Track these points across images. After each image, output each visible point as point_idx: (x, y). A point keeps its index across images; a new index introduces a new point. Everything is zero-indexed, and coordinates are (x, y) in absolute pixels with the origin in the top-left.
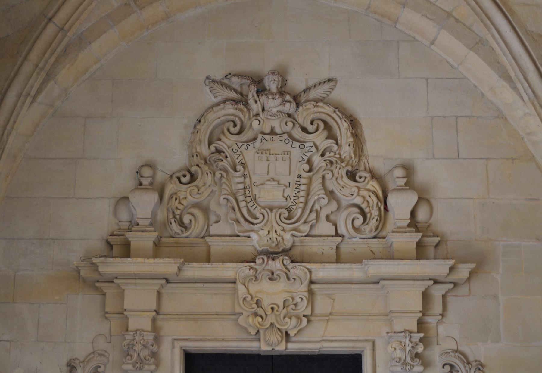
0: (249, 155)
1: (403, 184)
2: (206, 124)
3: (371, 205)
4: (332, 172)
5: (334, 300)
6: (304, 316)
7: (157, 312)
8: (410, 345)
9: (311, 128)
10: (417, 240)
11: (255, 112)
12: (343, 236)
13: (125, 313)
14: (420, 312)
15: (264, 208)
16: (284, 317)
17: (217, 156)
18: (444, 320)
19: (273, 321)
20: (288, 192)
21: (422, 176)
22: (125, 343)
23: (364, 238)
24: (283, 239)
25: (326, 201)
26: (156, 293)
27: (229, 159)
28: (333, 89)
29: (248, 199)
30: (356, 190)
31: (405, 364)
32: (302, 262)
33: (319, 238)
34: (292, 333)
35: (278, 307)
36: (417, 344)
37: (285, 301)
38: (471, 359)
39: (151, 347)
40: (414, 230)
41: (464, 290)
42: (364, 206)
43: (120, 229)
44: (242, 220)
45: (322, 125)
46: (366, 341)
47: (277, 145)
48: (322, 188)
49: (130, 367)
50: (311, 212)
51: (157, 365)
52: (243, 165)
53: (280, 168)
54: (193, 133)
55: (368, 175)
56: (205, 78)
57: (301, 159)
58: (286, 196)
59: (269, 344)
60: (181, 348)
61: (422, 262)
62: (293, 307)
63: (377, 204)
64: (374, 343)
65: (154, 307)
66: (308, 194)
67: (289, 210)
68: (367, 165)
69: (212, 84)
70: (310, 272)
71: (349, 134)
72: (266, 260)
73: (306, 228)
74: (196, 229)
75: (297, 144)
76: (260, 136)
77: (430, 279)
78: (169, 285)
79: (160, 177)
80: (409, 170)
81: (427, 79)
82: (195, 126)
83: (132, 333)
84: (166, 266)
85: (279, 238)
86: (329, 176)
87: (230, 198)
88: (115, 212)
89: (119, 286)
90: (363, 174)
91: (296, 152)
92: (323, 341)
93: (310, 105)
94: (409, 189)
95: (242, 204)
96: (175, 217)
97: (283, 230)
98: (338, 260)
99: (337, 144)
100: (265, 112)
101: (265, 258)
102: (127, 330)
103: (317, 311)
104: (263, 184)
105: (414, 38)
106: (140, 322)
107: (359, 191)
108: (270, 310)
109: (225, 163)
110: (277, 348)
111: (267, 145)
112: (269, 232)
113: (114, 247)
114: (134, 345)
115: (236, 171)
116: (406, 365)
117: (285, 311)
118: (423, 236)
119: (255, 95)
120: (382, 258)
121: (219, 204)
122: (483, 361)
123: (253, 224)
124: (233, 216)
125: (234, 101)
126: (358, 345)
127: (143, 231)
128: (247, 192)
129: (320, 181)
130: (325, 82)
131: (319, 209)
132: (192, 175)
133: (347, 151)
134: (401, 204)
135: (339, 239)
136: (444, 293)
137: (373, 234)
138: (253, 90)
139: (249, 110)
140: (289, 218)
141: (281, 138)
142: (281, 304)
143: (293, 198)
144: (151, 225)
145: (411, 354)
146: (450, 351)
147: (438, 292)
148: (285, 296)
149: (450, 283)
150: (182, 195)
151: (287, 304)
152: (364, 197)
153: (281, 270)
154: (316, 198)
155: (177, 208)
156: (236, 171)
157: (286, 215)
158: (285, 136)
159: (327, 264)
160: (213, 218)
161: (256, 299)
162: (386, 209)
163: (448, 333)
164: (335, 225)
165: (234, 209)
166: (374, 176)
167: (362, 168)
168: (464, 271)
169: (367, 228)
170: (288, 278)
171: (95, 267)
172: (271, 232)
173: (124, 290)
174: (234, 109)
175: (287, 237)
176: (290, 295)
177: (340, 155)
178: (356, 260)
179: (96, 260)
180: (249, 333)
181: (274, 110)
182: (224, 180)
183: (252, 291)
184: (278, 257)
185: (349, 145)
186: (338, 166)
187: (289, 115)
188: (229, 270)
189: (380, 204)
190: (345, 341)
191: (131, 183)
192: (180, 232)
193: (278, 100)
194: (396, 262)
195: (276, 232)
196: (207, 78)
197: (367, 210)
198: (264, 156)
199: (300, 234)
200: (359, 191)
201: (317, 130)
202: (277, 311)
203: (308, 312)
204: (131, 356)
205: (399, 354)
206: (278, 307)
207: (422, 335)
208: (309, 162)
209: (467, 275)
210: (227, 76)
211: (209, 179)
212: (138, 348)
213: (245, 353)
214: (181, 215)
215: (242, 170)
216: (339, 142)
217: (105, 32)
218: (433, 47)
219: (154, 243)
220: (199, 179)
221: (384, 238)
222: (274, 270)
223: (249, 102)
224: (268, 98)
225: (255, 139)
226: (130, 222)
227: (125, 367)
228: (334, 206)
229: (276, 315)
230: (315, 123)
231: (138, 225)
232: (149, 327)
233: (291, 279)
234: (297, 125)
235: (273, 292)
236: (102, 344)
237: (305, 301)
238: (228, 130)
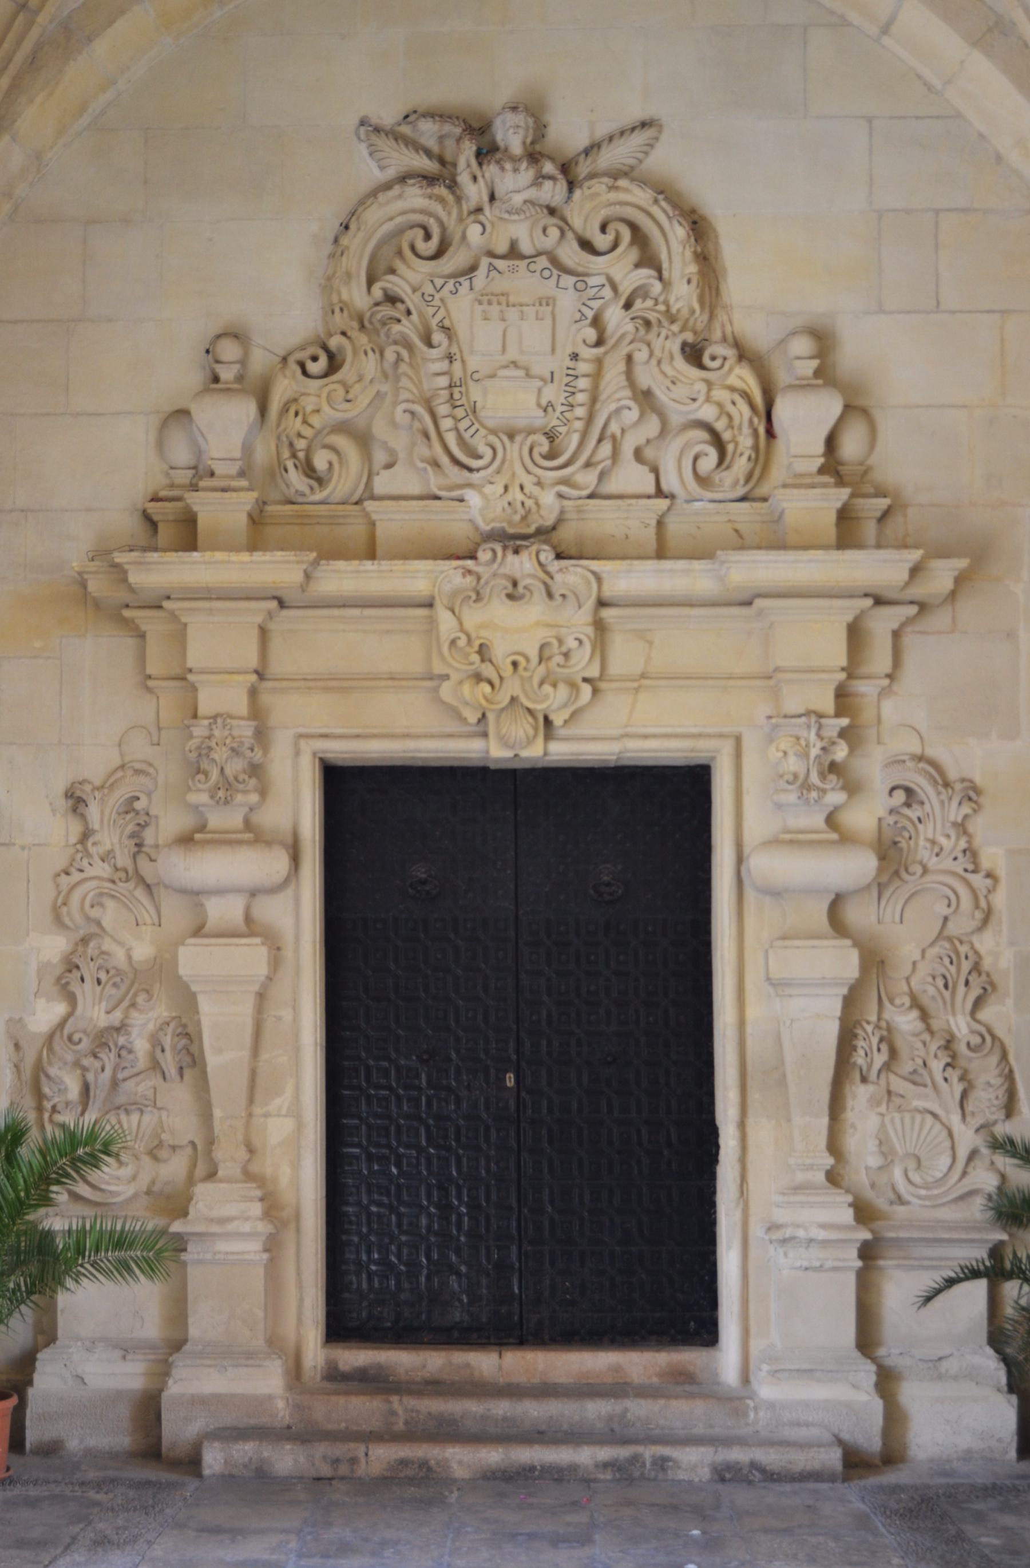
0: (461, 307)
1: (810, 372)
2: (361, 234)
3: (736, 422)
4: (649, 345)
5: (650, 643)
6: (585, 680)
7: (260, 675)
8: (819, 744)
9: (601, 241)
10: (839, 505)
11: (473, 204)
12: (672, 497)
13: (191, 677)
14: (843, 669)
15: (494, 432)
16: (541, 684)
17: (386, 310)
18: (895, 688)
19: (517, 691)
20: (550, 393)
21: (852, 354)
22: (193, 744)
23: (720, 501)
24: (537, 504)
25: (634, 414)
26: (255, 632)
27: (415, 317)
28: (651, 146)
29: (460, 413)
30: (702, 387)
31: (806, 786)
32: (580, 558)
33: (619, 502)
34: (558, 720)
35: (528, 660)
36: (834, 743)
37: (542, 647)
38: (953, 775)
39: (249, 754)
40: (832, 480)
41: (941, 619)
42: (720, 426)
43: (172, 486)
44: (445, 460)
45: (626, 234)
46: (721, 736)
47: (523, 282)
48: (625, 383)
49: (204, 798)
50: (600, 440)
51: (263, 792)
52: (446, 330)
53: (532, 337)
54: (332, 256)
55: (730, 353)
56: (356, 122)
57: (578, 316)
58: (544, 402)
59: (510, 744)
60: (314, 754)
61: (850, 554)
62: (559, 659)
63: (751, 421)
64: (738, 740)
65: (253, 662)
66: (594, 400)
67: (551, 436)
68: (728, 329)
69: (374, 138)
70: (599, 579)
71: (689, 254)
72: (500, 554)
73: (588, 479)
74: (344, 483)
75: (568, 281)
76: (485, 262)
77: (866, 595)
78: (285, 613)
79: (260, 361)
80: (823, 340)
81: (870, 120)
82: (336, 240)
83: (206, 722)
84: (278, 569)
85: (529, 503)
86: (641, 356)
87: (420, 409)
88: (160, 445)
89: (174, 617)
90: (720, 350)
91: (567, 301)
92: (627, 735)
93: (599, 186)
94: (825, 385)
95: (446, 424)
96: (294, 456)
97: (539, 483)
98: (661, 554)
99: (660, 278)
100: (497, 203)
101: (498, 548)
102: (195, 716)
103: (615, 668)
104: (493, 376)
105: (842, 17)
106: (224, 697)
107: (709, 390)
108: (510, 668)
109: (407, 328)
110: (525, 753)
111: (501, 284)
112: (506, 488)
113: (161, 527)
114: (210, 749)
115: (430, 344)
116: (809, 790)
117: (542, 670)
118: (853, 495)
119: (474, 163)
120: (759, 548)
121: (393, 424)
122: (978, 780)
123: (470, 470)
124: (423, 450)
125: (425, 177)
126: (702, 744)
127: (224, 490)
128: (457, 396)
129: (622, 367)
130: (633, 129)
131: (618, 433)
132: (331, 356)
133: (683, 294)
134: (805, 421)
135: (663, 504)
136: (895, 625)
137: (740, 491)
138: (469, 148)
139: (459, 199)
140: (551, 456)
141: (532, 267)
142: (533, 654)
143: (560, 409)
144: (242, 474)
145: (820, 764)
146: (905, 758)
147: (882, 624)
148: (543, 634)
149: (912, 603)
150: (308, 404)
151: (547, 653)
152: (720, 405)
153: (534, 576)
154: (613, 406)
155: (300, 435)
156: (430, 344)
157: (545, 447)
158: (543, 262)
159: (636, 562)
160: (380, 457)
161: (477, 643)
162: (770, 433)
163: (904, 718)
164: (655, 470)
165: (427, 436)
166: (744, 354)
167: (718, 335)
168: (942, 576)
169: (727, 477)
170: (550, 595)
171: (119, 573)
172: (510, 489)
173: (185, 625)
174: (424, 196)
175: (548, 498)
176: (553, 632)
177: (668, 306)
178: (702, 551)
179: (120, 558)
180: (464, 720)
181: (518, 199)
182: (404, 368)
183: (469, 623)
184: (527, 547)
185: (689, 282)
186: (664, 332)
187: (552, 211)
188: (417, 578)
189: (756, 420)
190: (676, 736)
191: (196, 378)
192: (307, 491)
193: (526, 174)
194: (791, 555)
195: (522, 488)
196: (363, 123)
197: (726, 436)
198: (494, 310)
199: (575, 493)
200: (709, 390)
201: (615, 246)
202: (525, 669)
203: (594, 672)
204: (206, 774)
205: (793, 764)
206: (528, 660)
207: (845, 722)
208: (597, 322)
209: (948, 584)
210: (406, 117)
211: (370, 365)
212: (220, 754)
213: (456, 764)
214: (308, 451)
215: (445, 342)
216: (665, 274)
217: (122, 12)
218: (886, 40)
219: (250, 516)
221: (765, 500)
222: (518, 575)
223: (459, 179)
224: (502, 169)
225: (473, 268)
226: (195, 468)
227: (193, 798)
228: (652, 426)
229: (522, 679)
230: (611, 228)
231: (212, 474)
232: (243, 709)
233: (557, 596)
234: (570, 235)
235: (516, 627)
236: (139, 749)
237: (588, 646)
238: (413, 248)
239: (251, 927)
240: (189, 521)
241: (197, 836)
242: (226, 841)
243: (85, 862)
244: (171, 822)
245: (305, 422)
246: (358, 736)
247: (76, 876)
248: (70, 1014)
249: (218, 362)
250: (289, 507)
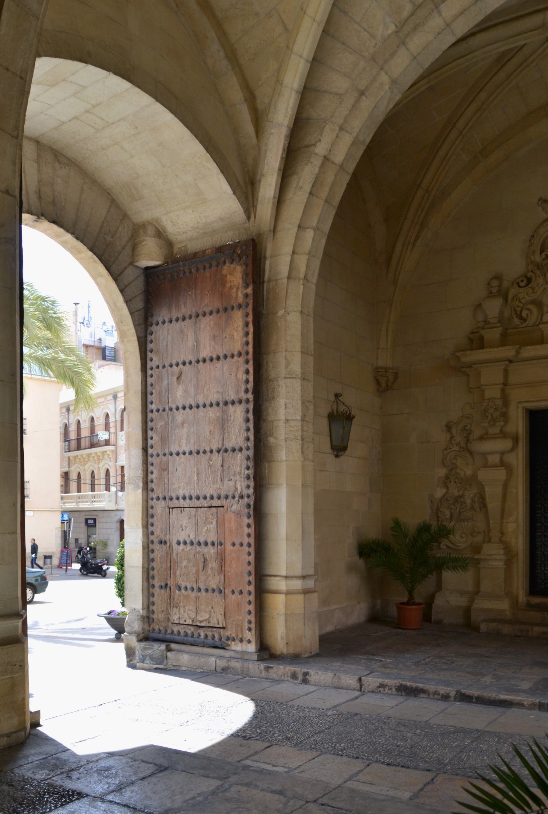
60: (523, 408)
65: (501, 379)
74: (531, 321)
78: (512, 364)
96: (516, 313)
144: (499, 321)
155: (518, 306)
220: (533, 282)
239: (502, 464)
240: (482, 338)
241: (485, 436)
242: (494, 437)
243: (451, 446)
244: (477, 433)
245: (520, 302)
246: (538, 401)
247: (449, 451)
248: (447, 492)
249: (492, 287)
250: (515, 330)
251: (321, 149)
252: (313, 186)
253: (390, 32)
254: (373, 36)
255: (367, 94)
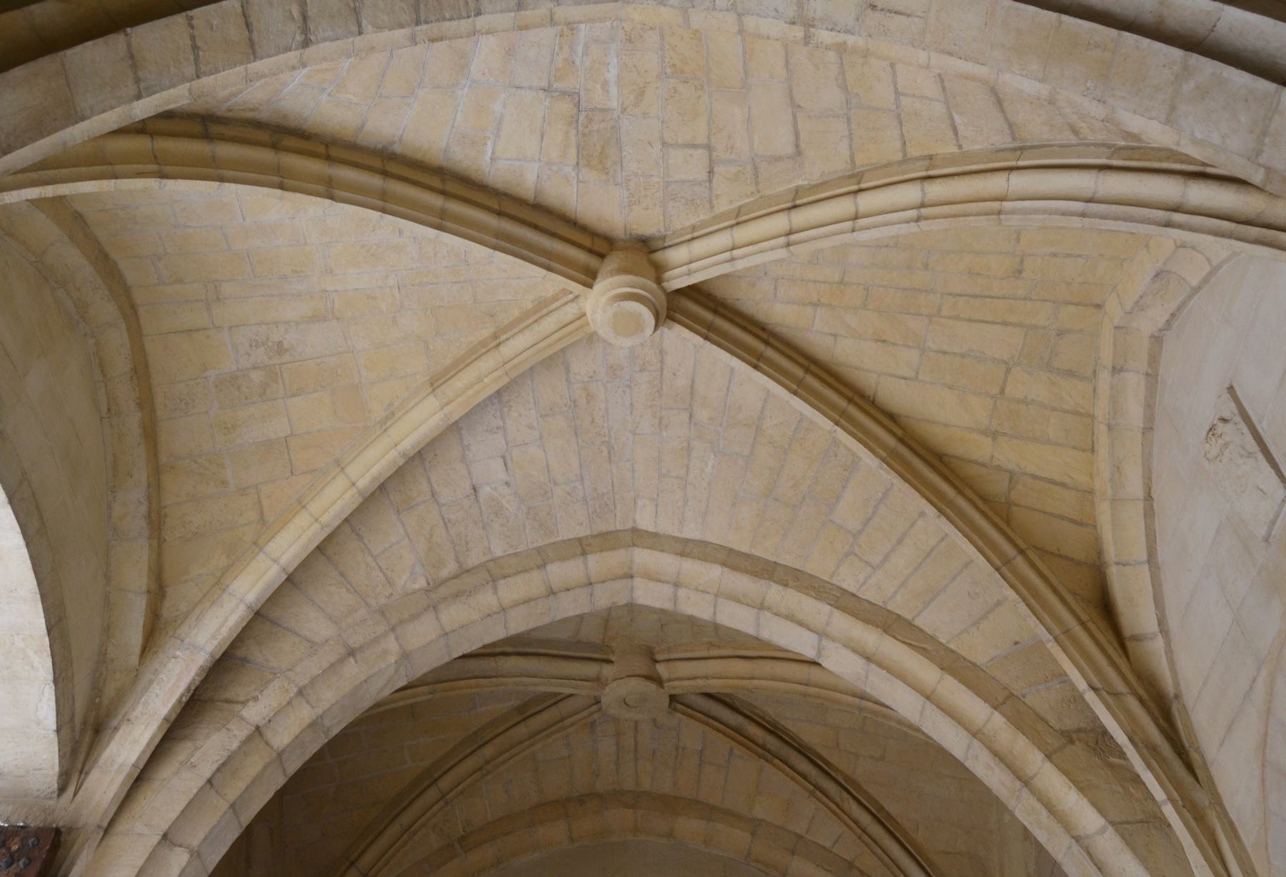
251: (254, 713)
252: (218, 770)
253: (417, 586)
254: (390, 582)
255: (358, 656)
